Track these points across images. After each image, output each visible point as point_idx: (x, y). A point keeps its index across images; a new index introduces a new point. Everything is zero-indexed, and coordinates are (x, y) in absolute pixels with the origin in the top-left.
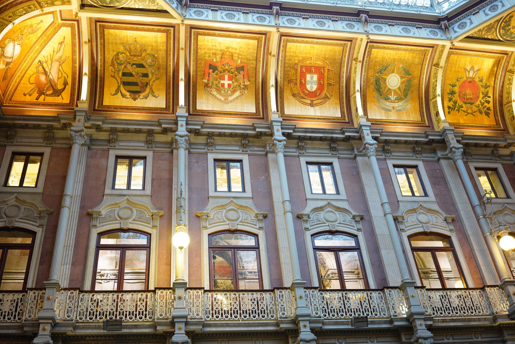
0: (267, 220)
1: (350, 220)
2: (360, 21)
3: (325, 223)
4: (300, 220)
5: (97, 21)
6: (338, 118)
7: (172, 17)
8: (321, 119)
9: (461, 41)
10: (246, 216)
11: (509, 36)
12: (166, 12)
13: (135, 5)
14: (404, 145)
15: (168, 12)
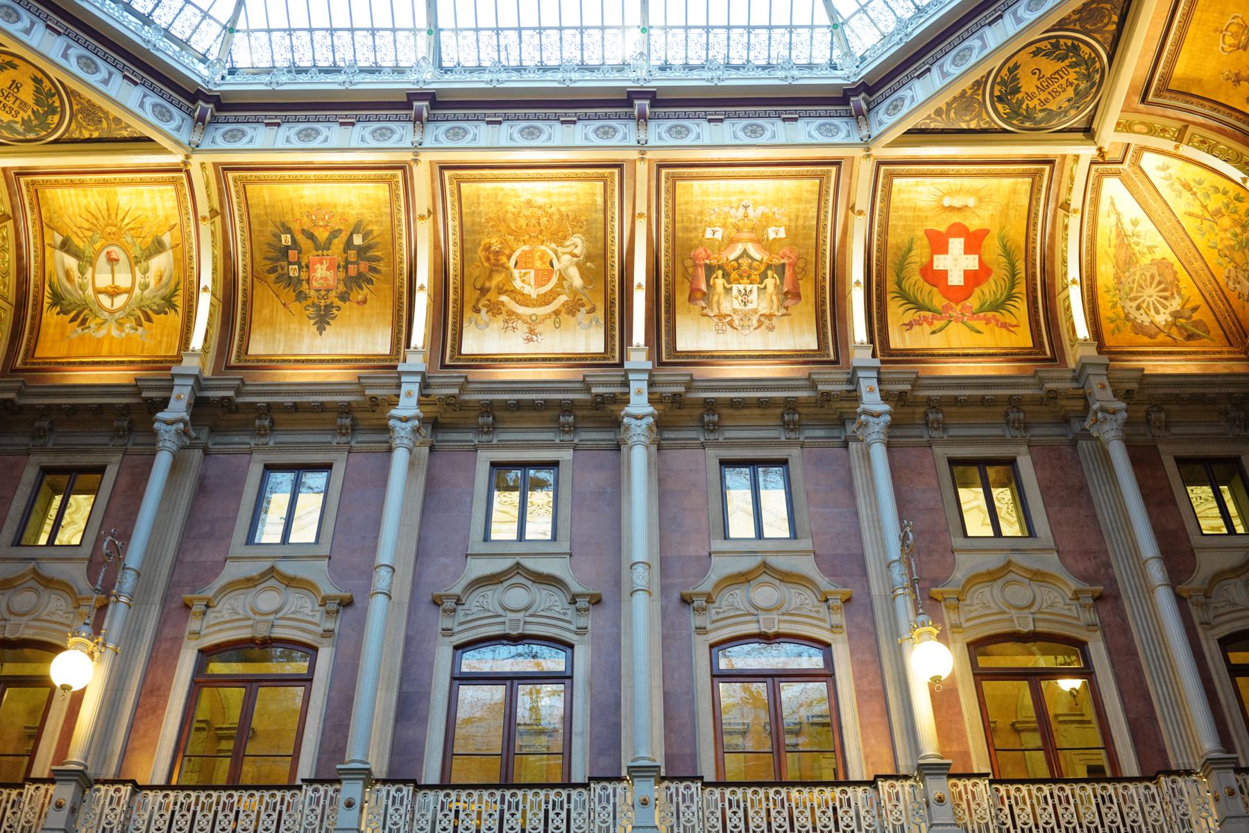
0: (350, 612)
1: (567, 606)
2: (630, 117)
3: (501, 616)
4: (435, 607)
5: (22, 172)
6: (594, 356)
7: (163, 150)
8: (550, 360)
9: (895, 144)
10: (299, 602)
11: (1029, 117)
12: (149, 140)
13: (81, 132)
14: (757, 411)
15: (153, 141)
